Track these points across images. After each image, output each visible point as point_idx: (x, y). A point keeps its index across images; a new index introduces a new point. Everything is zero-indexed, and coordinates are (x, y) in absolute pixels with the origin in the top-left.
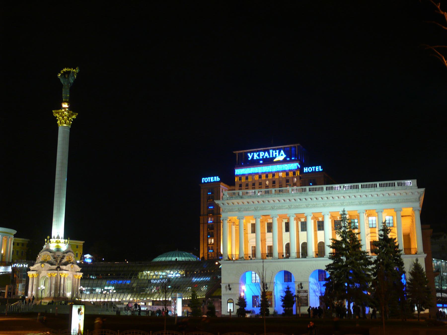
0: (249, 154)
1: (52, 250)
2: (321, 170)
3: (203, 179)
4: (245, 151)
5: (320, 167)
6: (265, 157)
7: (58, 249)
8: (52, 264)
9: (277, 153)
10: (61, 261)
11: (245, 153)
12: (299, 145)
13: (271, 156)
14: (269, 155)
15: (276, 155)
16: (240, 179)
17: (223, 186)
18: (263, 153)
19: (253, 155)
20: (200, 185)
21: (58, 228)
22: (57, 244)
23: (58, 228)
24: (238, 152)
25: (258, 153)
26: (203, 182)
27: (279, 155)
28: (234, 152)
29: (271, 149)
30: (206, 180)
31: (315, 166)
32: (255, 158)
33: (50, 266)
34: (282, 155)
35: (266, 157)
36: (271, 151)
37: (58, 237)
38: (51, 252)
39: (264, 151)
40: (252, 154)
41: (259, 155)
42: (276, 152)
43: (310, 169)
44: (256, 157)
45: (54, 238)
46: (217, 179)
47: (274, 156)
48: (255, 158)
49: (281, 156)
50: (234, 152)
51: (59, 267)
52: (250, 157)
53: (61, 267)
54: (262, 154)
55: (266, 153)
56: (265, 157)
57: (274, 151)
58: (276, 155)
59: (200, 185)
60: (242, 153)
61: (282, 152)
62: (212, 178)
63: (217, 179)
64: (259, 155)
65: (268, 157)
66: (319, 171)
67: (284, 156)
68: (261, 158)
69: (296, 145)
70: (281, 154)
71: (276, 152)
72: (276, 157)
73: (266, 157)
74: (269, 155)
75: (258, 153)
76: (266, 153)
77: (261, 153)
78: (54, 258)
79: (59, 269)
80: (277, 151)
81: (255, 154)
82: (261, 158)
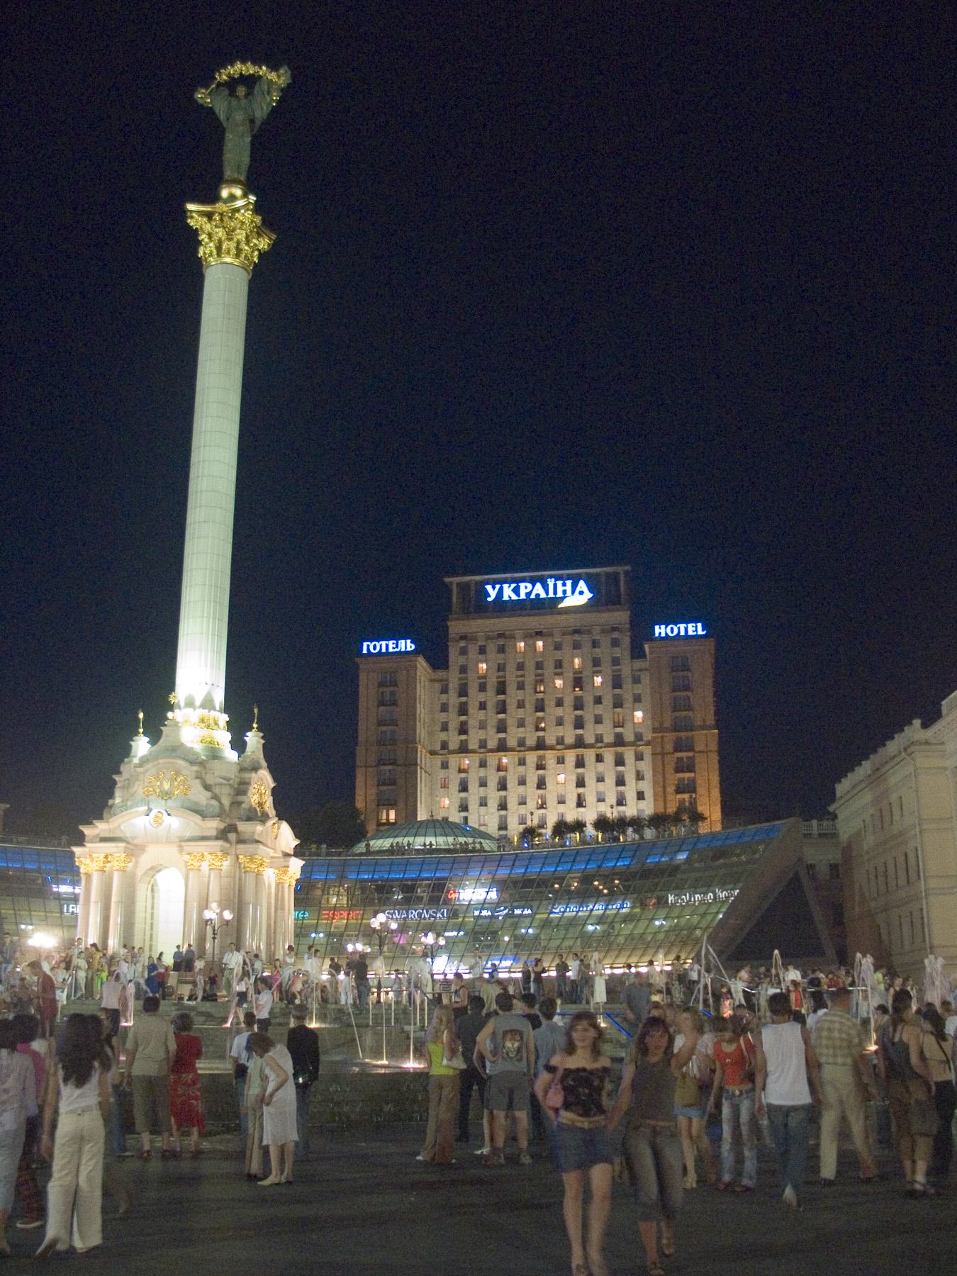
0: (489, 588)
1: (195, 753)
2: (700, 632)
3: (365, 644)
4: (478, 578)
5: (699, 625)
6: (533, 596)
7: (214, 754)
8: (203, 815)
10: (236, 804)
11: (477, 583)
12: (628, 568)
13: (551, 595)
14: (547, 593)
15: (565, 592)
16: (464, 651)
17: (421, 662)
18: (530, 586)
19: (501, 589)
20: (357, 660)
21: (200, 665)
22: (206, 732)
23: (200, 665)
24: (454, 580)
25: (513, 585)
26: (365, 651)
27: (573, 593)
28: (447, 580)
29: (551, 577)
30: (375, 647)
31: (687, 623)
32: (506, 598)
34: (581, 593)
35: (538, 595)
36: (551, 582)
37: (208, 704)
38: (192, 763)
40: (498, 587)
41: (516, 591)
42: (564, 585)
43: (672, 630)
44: (508, 593)
45: (190, 704)
47: (560, 594)
48: (506, 598)
49: (577, 596)
50: (447, 580)
51: (232, 828)
52: (492, 593)
53: (243, 827)
54: (525, 588)
55: (538, 585)
56: (533, 596)
57: (559, 583)
58: (565, 592)
59: (357, 660)
60: (467, 585)
61: (582, 585)
62: (391, 644)
63: (407, 645)
64: (516, 591)
65: (543, 595)
66: (697, 636)
67: (588, 594)
68: (523, 596)
69: (620, 569)
70: (578, 589)
71: (564, 585)
72: (562, 599)
73: (538, 595)
74: (547, 593)
75: (513, 585)
76: (538, 585)
77: (522, 585)
78: (207, 787)
79: (232, 836)
80: (569, 583)
81: (506, 586)
82: (523, 596)
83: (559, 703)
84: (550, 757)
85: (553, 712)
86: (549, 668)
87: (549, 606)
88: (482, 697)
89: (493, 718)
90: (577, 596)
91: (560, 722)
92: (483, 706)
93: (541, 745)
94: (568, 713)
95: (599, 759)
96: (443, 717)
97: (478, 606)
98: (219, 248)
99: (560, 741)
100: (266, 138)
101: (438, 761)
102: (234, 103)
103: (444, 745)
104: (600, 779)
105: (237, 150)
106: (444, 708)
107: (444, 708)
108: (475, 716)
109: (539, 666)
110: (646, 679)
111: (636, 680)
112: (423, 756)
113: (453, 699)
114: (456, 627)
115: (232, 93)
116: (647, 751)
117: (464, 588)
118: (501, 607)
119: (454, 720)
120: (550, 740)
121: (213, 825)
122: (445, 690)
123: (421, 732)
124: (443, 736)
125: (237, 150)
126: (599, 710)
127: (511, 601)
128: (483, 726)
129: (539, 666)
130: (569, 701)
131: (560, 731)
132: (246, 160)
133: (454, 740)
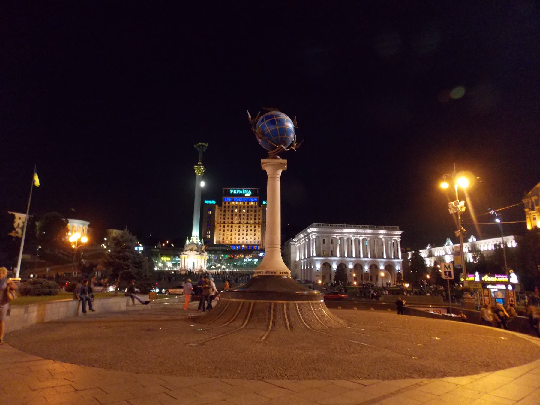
16: (225, 203)
17: (217, 206)
24: (224, 189)
39: (240, 190)
44: (235, 192)
46: (214, 202)
49: (248, 193)
52: (231, 192)
61: (250, 191)
63: (214, 202)
69: (258, 189)
83: (244, 215)
84: (241, 226)
85: (242, 217)
86: (242, 208)
87: (242, 195)
88: (228, 213)
89: (230, 217)
90: (248, 193)
91: (244, 219)
92: (228, 215)
93: (240, 223)
94: (245, 217)
95: (251, 227)
96: (220, 216)
97: (228, 194)
99: (244, 223)
101: (219, 225)
103: (220, 222)
104: (251, 230)
105: (200, 156)
106: (221, 215)
107: (221, 215)
108: (227, 217)
109: (240, 207)
110: (261, 211)
111: (259, 211)
112: (216, 224)
113: (223, 213)
114: (224, 198)
116: (260, 226)
117: (226, 190)
118: (233, 195)
119: (222, 217)
120: (242, 222)
122: (221, 211)
123: (216, 219)
124: (220, 220)
125: (200, 156)
126: (252, 217)
128: (228, 219)
129: (240, 207)
130: (246, 215)
131: (244, 221)
133: (222, 221)
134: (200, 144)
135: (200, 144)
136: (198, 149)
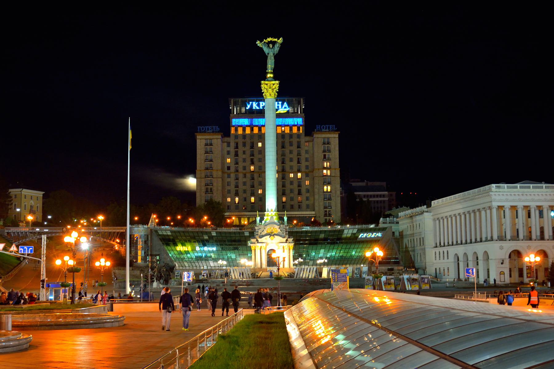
9: (280, 106)
15: (278, 107)
19: (252, 104)
27: (282, 107)
32: (254, 108)
33: (281, 238)
34: (285, 108)
40: (251, 103)
41: (258, 105)
42: (278, 104)
48: (254, 108)
58: (278, 107)
61: (285, 104)
64: (258, 105)
68: (261, 108)
70: (284, 106)
80: (280, 103)
81: (254, 103)
98: (270, 95)
100: (276, 57)
102: (270, 50)
105: (270, 65)
115: (269, 46)
121: (284, 240)
125: (270, 65)
127: (256, 109)
132: (273, 66)
134: (269, 39)
135: (269, 39)
136: (266, 50)
